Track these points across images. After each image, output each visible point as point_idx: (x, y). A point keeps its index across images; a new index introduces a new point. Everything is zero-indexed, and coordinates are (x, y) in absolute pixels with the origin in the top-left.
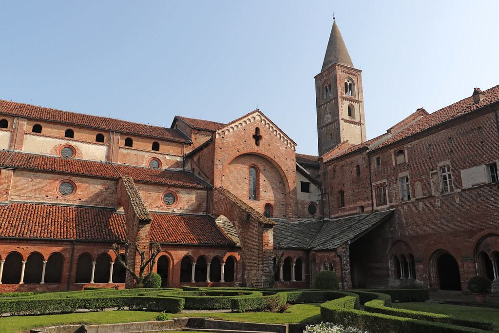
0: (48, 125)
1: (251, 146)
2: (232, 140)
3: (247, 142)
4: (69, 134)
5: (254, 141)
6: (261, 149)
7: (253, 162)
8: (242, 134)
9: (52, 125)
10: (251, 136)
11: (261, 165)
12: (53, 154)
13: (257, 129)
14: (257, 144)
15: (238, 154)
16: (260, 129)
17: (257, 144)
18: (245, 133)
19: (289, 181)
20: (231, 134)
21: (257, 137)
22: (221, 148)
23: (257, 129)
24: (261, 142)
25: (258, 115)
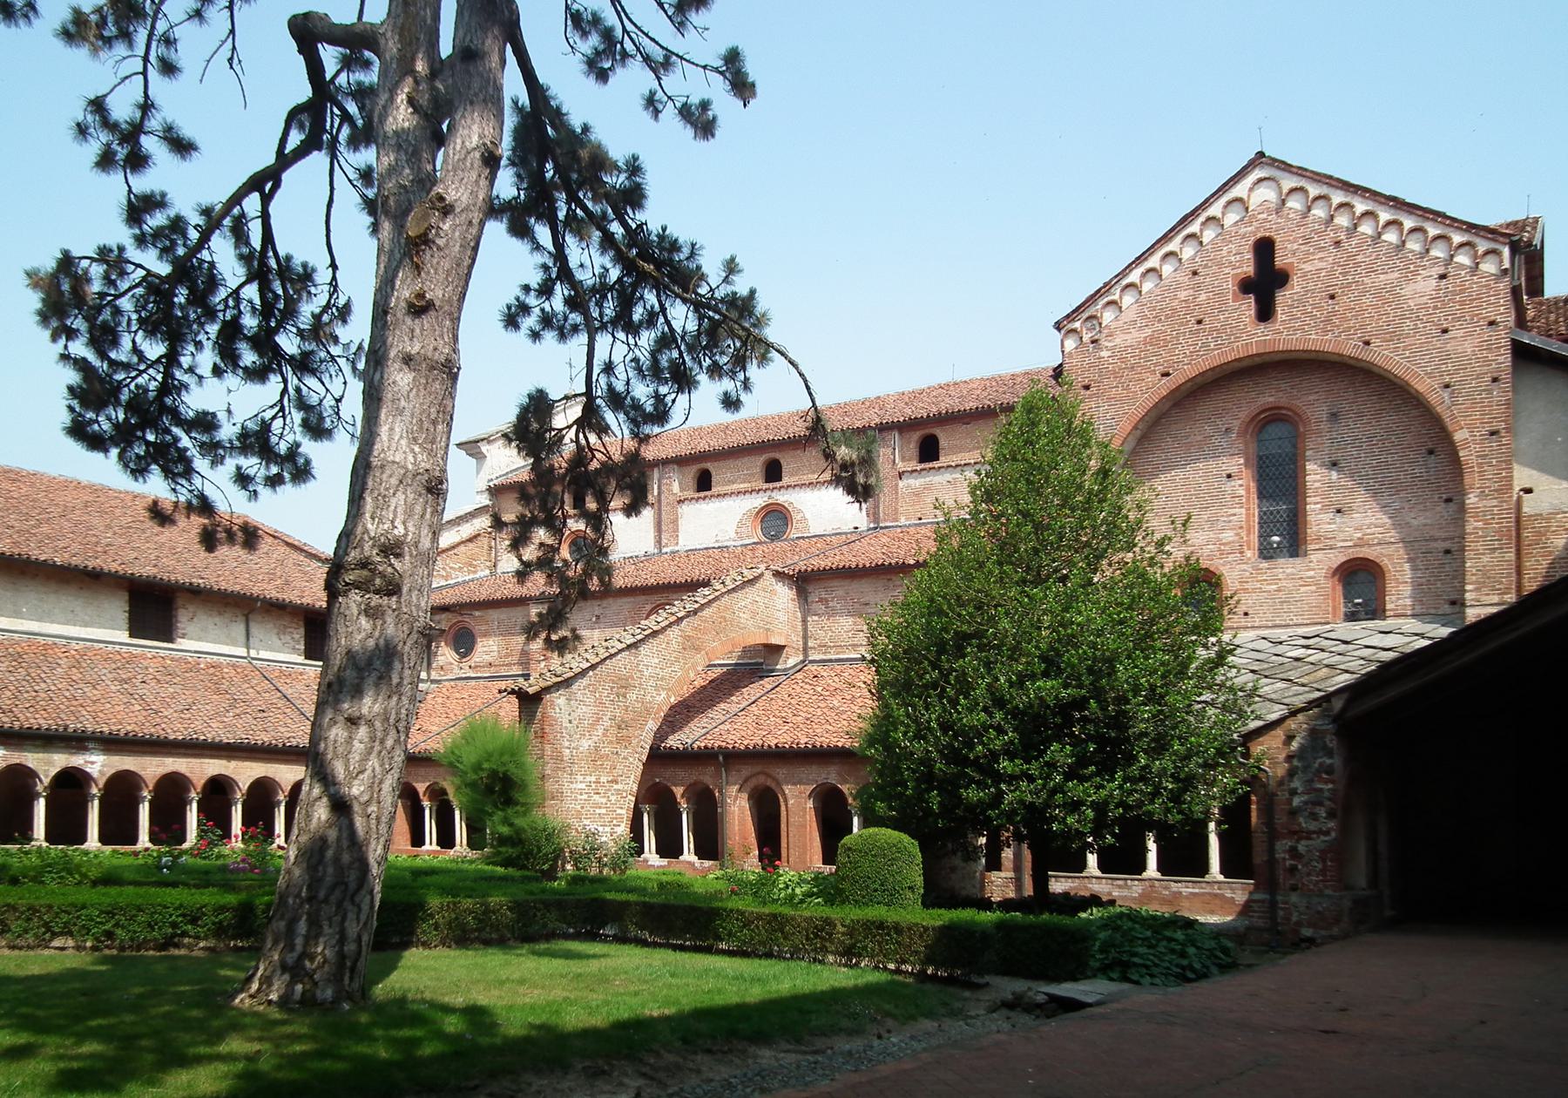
0: (721, 464)
1: (1242, 333)
2: (1135, 336)
3: (1206, 325)
4: (773, 473)
5: (1249, 305)
6: (1297, 326)
7: (1268, 399)
8: (1183, 295)
9: (731, 463)
10: (1231, 286)
11: (1313, 403)
12: (741, 538)
13: (1264, 249)
14: (1265, 313)
15: (1165, 387)
16: (1278, 239)
17: (1265, 313)
18: (1197, 288)
19: (1459, 436)
20: (1129, 315)
21: (1265, 282)
22: (1087, 387)
23: (1264, 249)
24: (1283, 298)
25: (1260, 180)
